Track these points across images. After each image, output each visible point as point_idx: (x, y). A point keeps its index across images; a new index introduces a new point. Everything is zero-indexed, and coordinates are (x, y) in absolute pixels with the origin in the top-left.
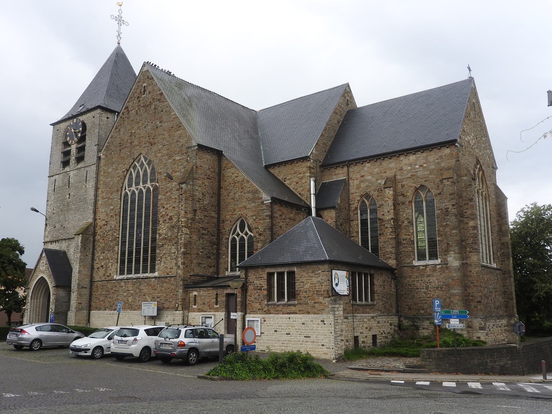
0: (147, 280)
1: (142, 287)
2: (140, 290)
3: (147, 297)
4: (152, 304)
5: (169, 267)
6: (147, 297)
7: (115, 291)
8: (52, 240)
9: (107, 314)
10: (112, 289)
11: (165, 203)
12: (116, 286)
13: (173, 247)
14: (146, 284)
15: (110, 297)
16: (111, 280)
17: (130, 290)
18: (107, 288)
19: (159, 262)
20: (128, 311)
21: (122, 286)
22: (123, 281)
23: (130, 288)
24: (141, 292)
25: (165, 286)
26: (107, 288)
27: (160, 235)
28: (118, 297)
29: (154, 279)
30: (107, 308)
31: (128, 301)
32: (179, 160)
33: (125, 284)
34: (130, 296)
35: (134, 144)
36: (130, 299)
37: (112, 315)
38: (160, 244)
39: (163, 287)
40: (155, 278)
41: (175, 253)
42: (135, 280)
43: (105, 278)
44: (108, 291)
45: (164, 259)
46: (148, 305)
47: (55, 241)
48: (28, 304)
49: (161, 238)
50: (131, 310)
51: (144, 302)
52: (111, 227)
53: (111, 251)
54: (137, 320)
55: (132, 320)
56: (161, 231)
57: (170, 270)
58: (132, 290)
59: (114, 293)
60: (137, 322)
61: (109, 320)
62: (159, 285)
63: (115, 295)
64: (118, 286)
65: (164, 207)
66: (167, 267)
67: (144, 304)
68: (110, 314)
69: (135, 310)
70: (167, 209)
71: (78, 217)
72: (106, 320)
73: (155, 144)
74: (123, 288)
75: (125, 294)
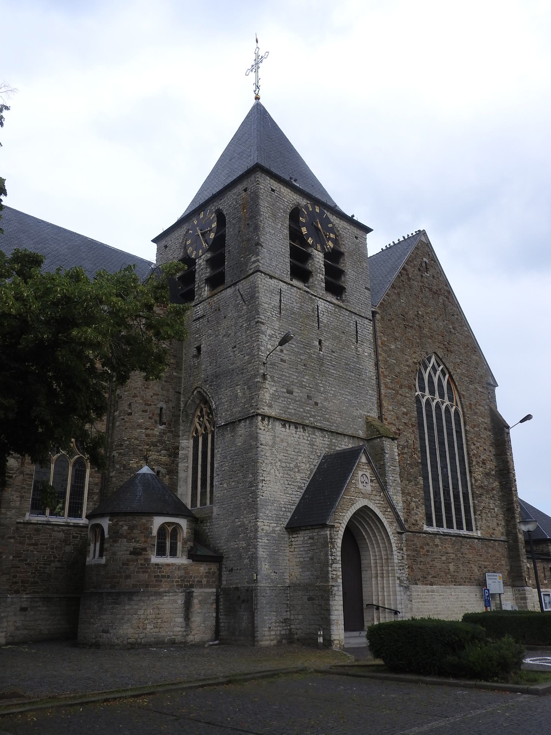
0: (468, 540)
1: (465, 550)
2: (462, 554)
3: (473, 566)
4: (497, 576)
5: (491, 527)
6: (473, 566)
7: (428, 551)
8: (284, 416)
9: (423, 592)
10: (422, 548)
11: (475, 439)
12: (428, 544)
13: (491, 501)
14: (468, 546)
15: (421, 562)
16: (419, 533)
17: (450, 553)
18: (414, 545)
19: (480, 517)
20: (451, 586)
21: (437, 546)
22: (438, 536)
23: (450, 550)
24: (464, 557)
25: (490, 551)
26: (414, 545)
27: (476, 481)
28: (434, 562)
29: (476, 541)
30: (419, 580)
31: (449, 570)
32: (481, 392)
33: (442, 543)
34: (451, 563)
35: (424, 332)
36: (452, 567)
37: (431, 593)
38: (477, 492)
39: (489, 553)
40: (479, 539)
41: (494, 509)
42: (454, 538)
43: (409, 527)
44: (416, 551)
45: (484, 515)
46: (493, 577)
47: (296, 425)
48: (334, 565)
49: (477, 484)
50: (455, 585)
51: (489, 574)
52: (407, 441)
53: (413, 483)
54: (468, 601)
55: (461, 601)
56: (475, 475)
57: (492, 531)
58: (452, 553)
59: (427, 555)
60: (469, 604)
61: (428, 602)
62: (484, 551)
63: (429, 559)
64: (431, 544)
65: (474, 444)
66: (488, 527)
67: (488, 576)
68: (428, 591)
69: (460, 585)
70: (478, 448)
71: (349, 397)
72: (422, 602)
73: (451, 352)
74: (440, 547)
75: (444, 558)
